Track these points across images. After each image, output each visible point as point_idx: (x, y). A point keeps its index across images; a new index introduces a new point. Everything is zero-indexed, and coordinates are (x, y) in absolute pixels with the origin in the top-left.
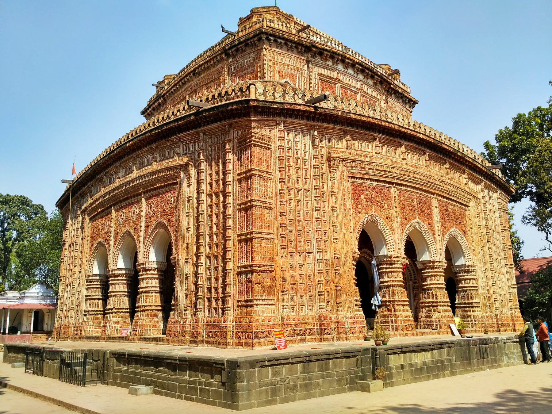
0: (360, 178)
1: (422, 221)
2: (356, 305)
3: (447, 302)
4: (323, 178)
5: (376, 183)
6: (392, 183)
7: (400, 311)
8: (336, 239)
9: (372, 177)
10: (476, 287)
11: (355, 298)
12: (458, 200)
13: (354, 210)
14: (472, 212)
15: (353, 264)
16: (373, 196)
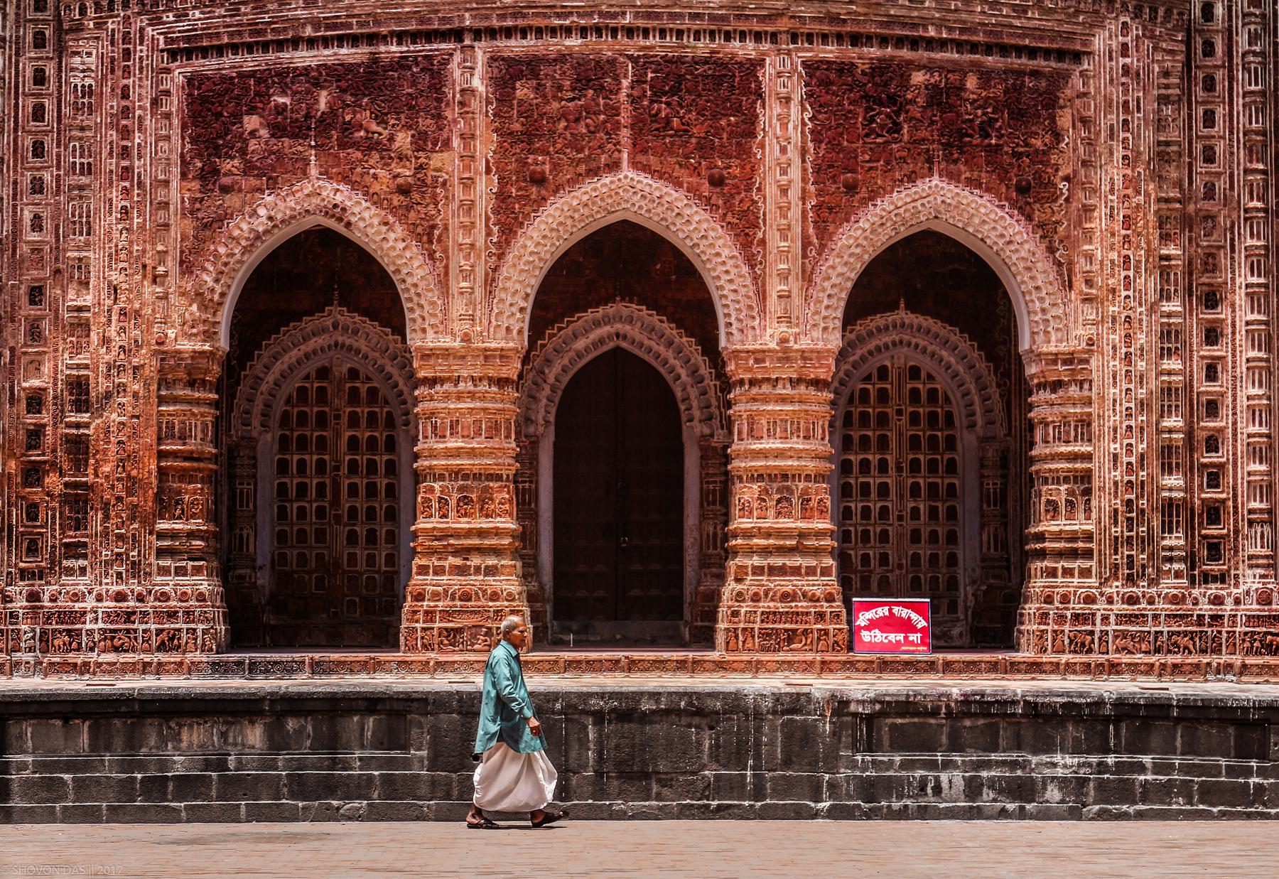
0: (235, 48)
1: (660, 175)
2: (161, 553)
3: (802, 535)
4: (40, 78)
5: (344, 51)
6: (457, 35)
7: (439, 571)
8: (79, 309)
9: (308, 31)
10: (1088, 457)
11: (163, 525)
12: (980, 38)
13: (195, 185)
14: (1101, 86)
15: (175, 400)
16: (323, 105)
